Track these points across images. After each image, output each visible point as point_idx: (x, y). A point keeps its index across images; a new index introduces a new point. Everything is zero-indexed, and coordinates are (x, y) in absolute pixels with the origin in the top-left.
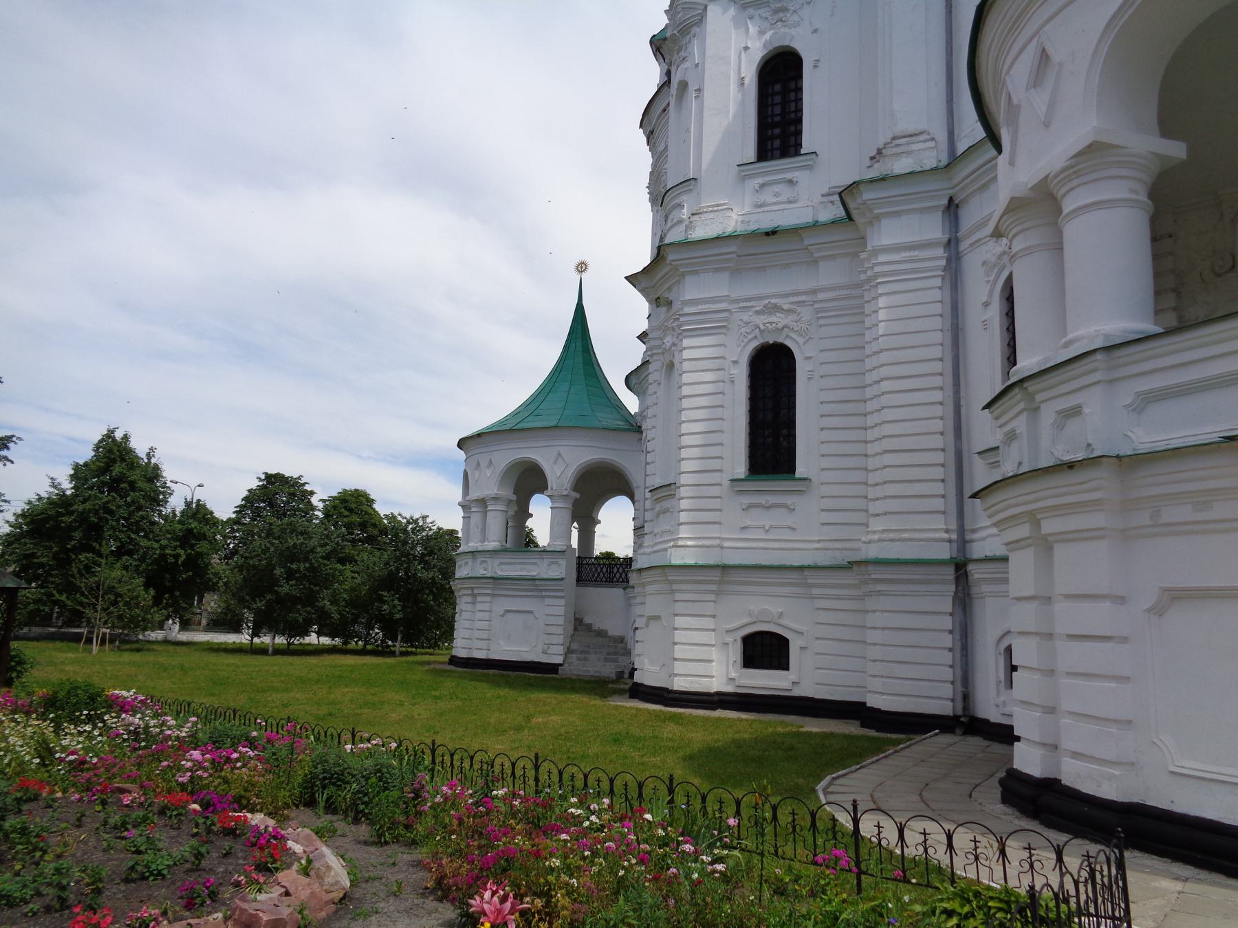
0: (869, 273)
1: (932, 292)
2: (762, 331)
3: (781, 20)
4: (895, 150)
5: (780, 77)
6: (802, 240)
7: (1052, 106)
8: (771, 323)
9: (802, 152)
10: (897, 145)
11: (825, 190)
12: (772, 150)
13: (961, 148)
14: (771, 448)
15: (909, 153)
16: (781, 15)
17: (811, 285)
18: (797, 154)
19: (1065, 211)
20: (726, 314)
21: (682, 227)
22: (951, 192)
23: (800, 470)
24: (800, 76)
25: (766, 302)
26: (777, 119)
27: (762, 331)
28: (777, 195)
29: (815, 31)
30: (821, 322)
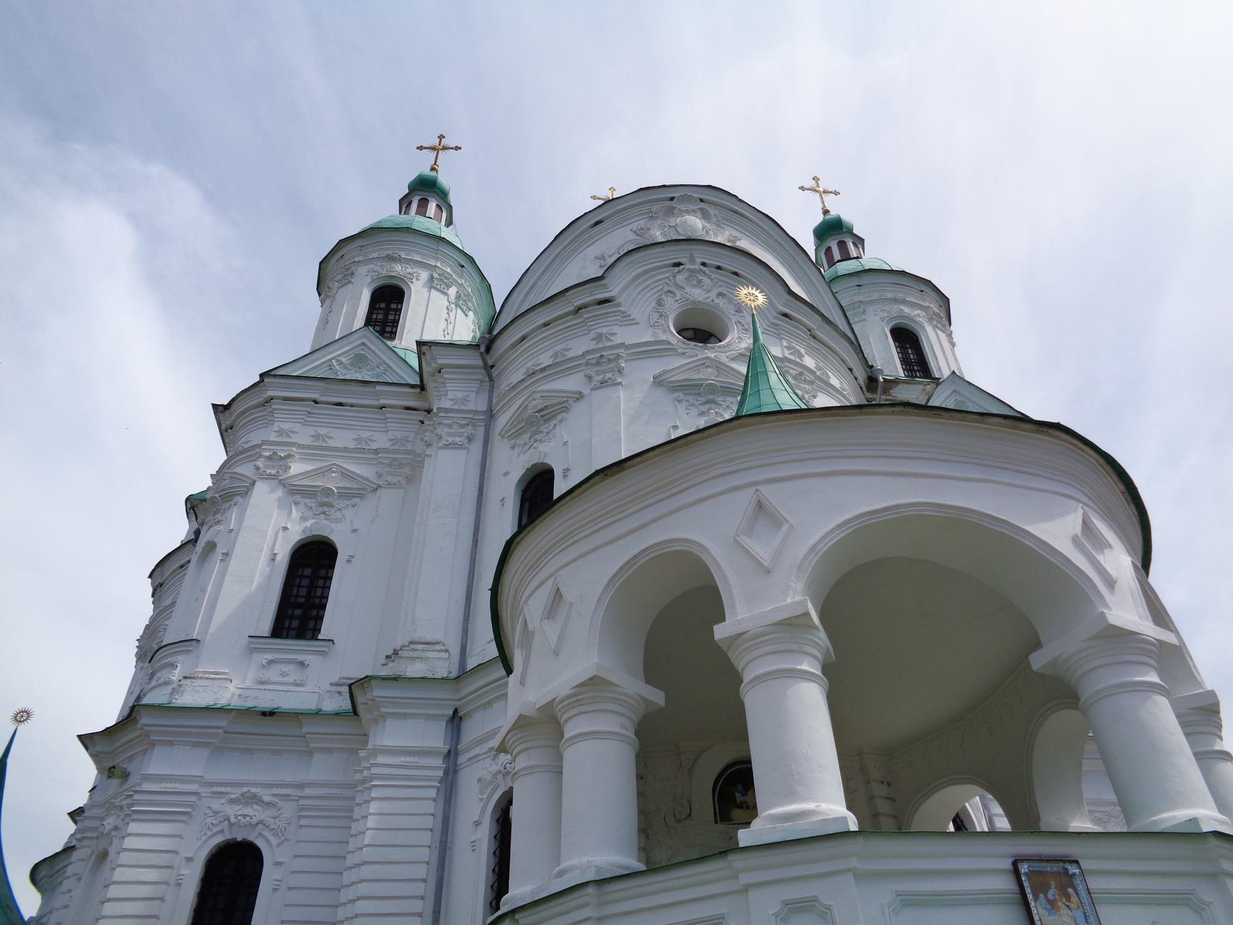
0: (366, 773)
1: (426, 804)
2: (231, 825)
3: (324, 513)
4: (411, 654)
6: (301, 727)
7: (562, 637)
8: (245, 816)
9: (320, 637)
10: (414, 650)
11: (335, 679)
12: (289, 629)
13: (471, 664)
16: (326, 509)
17: (299, 778)
18: (314, 637)
19: (567, 736)
20: (193, 798)
21: (169, 689)
22: (457, 704)
24: (332, 566)
25: (245, 789)
26: (302, 600)
27: (231, 825)
28: (283, 674)
29: (355, 531)
30: (303, 822)
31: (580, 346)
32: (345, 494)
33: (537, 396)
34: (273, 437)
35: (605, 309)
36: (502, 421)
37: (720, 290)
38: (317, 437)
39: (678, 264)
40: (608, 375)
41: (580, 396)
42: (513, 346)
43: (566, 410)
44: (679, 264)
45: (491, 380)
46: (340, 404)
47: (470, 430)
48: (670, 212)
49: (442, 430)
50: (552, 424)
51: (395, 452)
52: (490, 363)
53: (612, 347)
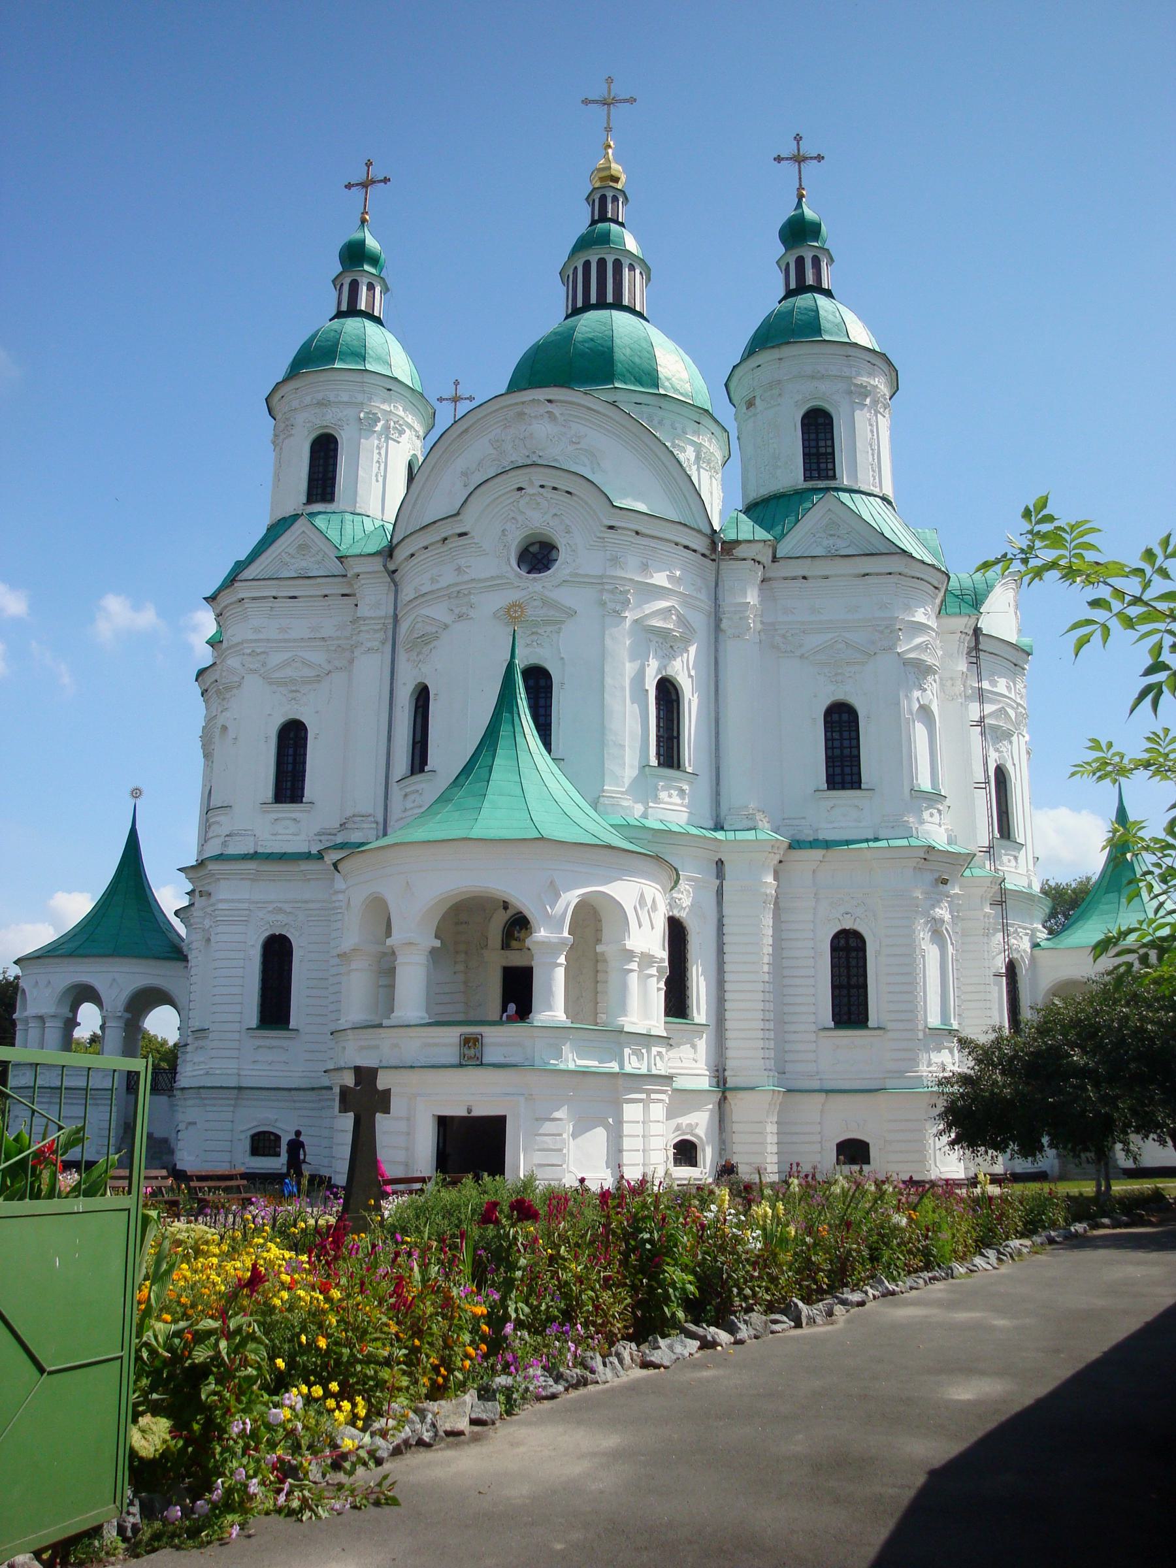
5: (292, 739)
11: (317, 829)
14: (275, 1008)
18: (302, 802)
23: (293, 1024)
33: (420, 619)
35: (463, 541)
36: (404, 627)
37: (554, 511)
39: (520, 489)
40: (464, 610)
41: (446, 626)
42: (406, 559)
44: (520, 489)
45: (396, 585)
46: (295, 597)
48: (521, 415)
50: (432, 646)
51: (338, 638)
52: (392, 567)
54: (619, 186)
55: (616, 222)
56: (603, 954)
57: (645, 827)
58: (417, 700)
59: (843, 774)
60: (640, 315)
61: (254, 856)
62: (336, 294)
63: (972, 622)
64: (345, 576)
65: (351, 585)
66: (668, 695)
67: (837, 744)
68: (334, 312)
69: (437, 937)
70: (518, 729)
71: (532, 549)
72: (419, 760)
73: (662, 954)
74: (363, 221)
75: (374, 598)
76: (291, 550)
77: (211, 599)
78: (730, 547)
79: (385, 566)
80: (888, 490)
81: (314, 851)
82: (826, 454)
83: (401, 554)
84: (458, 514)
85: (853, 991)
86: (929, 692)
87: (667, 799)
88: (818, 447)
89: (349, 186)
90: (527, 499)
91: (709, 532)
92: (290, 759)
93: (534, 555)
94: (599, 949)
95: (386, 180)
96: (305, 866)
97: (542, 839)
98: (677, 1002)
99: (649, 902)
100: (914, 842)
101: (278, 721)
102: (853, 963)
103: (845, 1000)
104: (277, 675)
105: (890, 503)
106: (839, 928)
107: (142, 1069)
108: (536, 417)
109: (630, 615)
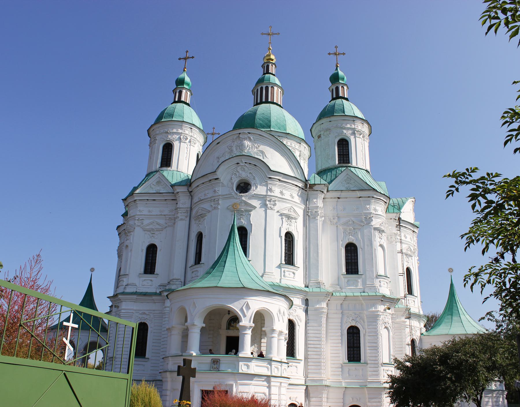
15: (176, 284)
23: (147, 356)
31: (210, 194)
32: (158, 230)
34: (138, 213)
35: (217, 181)
38: (149, 211)
41: (209, 211)
42: (196, 187)
43: (206, 216)
44: (238, 163)
47: (186, 214)
49: (179, 215)
51: (170, 215)
52: (190, 190)
53: (217, 196)
54: (273, 62)
55: (272, 74)
56: (264, 331)
57: (280, 286)
58: (198, 238)
59: (352, 269)
60: (280, 106)
61: (135, 293)
62: (174, 95)
63: (398, 215)
64: (173, 193)
65: (175, 196)
66: (289, 238)
67: (350, 258)
68: (173, 101)
69: (204, 323)
70: (235, 248)
71: (241, 185)
72: (198, 259)
73: (286, 331)
74: (184, 71)
75: (184, 201)
76: (155, 184)
77: (124, 200)
78: (312, 186)
79: (188, 190)
80: (368, 168)
81: (158, 292)
82: (346, 155)
83: (194, 185)
84: (215, 172)
85: (355, 349)
86: (383, 240)
87: (288, 276)
88: (343, 152)
89: (180, 59)
90: (240, 167)
91: (304, 180)
92: (151, 258)
93: (242, 187)
94: (263, 329)
95: (193, 57)
96: (154, 298)
97: (244, 287)
98: (291, 352)
99: (282, 312)
100: (378, 294)
101: (147, 244)
102: (355, 338)
103: (352, 353)
104: (148, 227)
105: (368, 172)
106: (350, 325)
107: (135, 327)
108: (244, 139)
109: (276, 208)
